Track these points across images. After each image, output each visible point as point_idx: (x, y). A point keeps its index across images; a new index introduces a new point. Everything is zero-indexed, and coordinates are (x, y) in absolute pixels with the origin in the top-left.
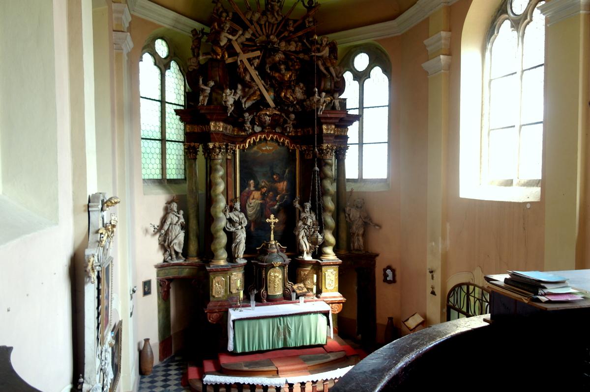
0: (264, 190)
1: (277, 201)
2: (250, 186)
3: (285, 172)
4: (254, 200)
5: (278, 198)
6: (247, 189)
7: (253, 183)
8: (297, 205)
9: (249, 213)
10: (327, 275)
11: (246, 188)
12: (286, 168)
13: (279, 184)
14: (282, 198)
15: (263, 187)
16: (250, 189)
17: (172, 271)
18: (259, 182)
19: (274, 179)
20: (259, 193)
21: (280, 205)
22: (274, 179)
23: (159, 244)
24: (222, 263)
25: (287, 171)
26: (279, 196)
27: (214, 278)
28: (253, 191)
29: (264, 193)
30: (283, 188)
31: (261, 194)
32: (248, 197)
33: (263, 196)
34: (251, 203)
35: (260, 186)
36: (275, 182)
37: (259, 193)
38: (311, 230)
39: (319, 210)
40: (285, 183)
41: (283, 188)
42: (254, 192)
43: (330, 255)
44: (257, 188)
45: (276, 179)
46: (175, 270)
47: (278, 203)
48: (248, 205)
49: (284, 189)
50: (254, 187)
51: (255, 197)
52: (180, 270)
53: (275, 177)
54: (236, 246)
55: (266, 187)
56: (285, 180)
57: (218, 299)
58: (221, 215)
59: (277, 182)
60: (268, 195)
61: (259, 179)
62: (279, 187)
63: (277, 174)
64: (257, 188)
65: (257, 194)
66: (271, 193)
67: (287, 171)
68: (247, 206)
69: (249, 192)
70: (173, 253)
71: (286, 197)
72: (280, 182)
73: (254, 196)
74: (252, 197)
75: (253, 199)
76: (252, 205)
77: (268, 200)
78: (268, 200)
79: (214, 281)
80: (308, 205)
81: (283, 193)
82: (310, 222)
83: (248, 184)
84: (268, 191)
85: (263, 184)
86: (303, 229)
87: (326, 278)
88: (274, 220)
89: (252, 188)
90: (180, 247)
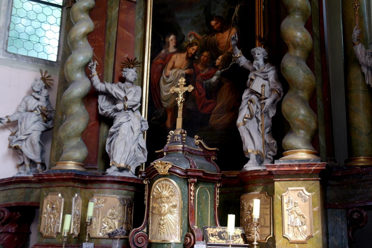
0: (192, 50)
1: (217, 68)
2: (169, 46)
3: (232, 11)
4: (174, 71)
5: (218, 62)
6: (163, 51)
7: (174, 40)
9: (165, 94)
10: (285, 200)
11: (161, 50)
12: (236, 5)
15: (191, 45)
16: (168, 51)
17: (18, 192)
18: (184, 36)
19: (211, 27)
20: (184, 55)
21: (222, 75)
22: (213, 27)
23: (10, 147)
24: (71, 166)
25: (237, 9)
26: (220, 57)
27: (47, 195)
28: (174, 53)
29: (193, 55)
31: (188, 58)
32: (164, 66)
33: (191, 60)
34: (168, 77)
35: (185, 44)
36: (212, 31)
37: (184, 55)
38: (264, 103)
39: (277, 53)
40: (234, 31)
42: (174, 56)
43: (301, 154)
44: (180, 48)
45: (215, 28)
46: (22, 191)
47: (218, 72)
48: (164, 81)
50: (176, 47)
51: (176, 64)
52: (28, 190)
53: (213, 23)
54: (111, 141)
55: (197, 45)
56: (233, 26)
57: (49, 241)
58: (79, 75)
59: (219, 32)
60: (199, 57)
61: (184, 33)
62: (221, 41)
63: (217, 17)
64: (180, 48)
65: (179, 59)
66: (205, 54)
67: (237, 9)
68: (161, 82)
69: (167, 55)
70: (27, 163)
72: (222, 32)
73: (174, 62)
74: (170, 65)
75: (173, 67)
76: (169, 80)
77: (199, 67)
78: (199, 67)
79: (45, 201)
82: (262, 86)
83: (164, 42)
84: (201, 50)
85: (191, 40)
87: (285, 207)
88: (186, 89)
89: (172, 49)
90: (34, 151)
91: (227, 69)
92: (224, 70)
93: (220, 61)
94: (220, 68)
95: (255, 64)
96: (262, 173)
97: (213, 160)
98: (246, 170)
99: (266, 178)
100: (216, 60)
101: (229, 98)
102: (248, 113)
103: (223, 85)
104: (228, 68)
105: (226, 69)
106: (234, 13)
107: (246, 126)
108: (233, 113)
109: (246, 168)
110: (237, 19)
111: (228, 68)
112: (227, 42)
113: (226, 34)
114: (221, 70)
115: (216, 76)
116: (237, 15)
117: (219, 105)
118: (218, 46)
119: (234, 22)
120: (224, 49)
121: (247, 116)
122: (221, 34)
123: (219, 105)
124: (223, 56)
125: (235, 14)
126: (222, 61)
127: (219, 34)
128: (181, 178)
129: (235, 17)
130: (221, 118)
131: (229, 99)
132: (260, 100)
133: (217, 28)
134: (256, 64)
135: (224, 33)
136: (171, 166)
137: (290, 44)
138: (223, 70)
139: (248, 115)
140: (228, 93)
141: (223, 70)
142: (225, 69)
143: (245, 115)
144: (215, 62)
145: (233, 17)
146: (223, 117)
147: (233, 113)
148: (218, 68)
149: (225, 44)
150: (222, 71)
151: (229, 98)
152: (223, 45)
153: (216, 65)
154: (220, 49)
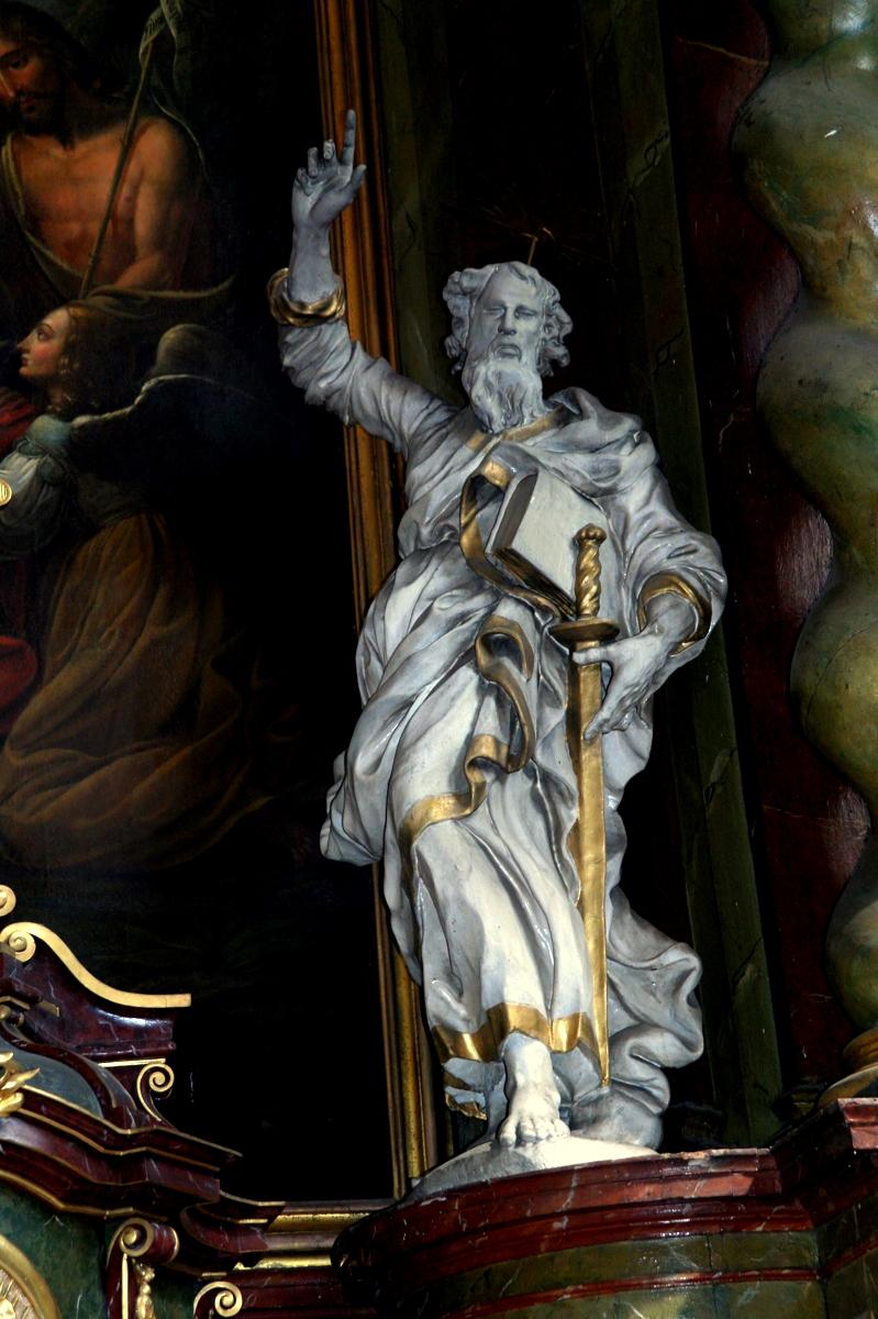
1: (34, 395)
5: (39, 350)
8: (341, 368)
13: (49, 157)
14: (111, 353)
21: (78, 453)
26: (58, 319)
30: (118, 222)
38: (609, 672)
40: (156, 145)
41: (118, 222)
47: (47, 427)
49: (143, 227)
56: (150, 110)
59: (38, 129)
62: (63, 199)
71: (170, 337)
80: (518, 306)
81: (129, 279)
82: (579, 543)
86: (465, 656)
91: (118, 413)
92: (96, 418)
93: (55, 344)
94: (59, 396)
95: (488, 385)
96: (700, 1183)
97: (155, 1094)
98: (524, 1161)
99: (716, 1229)
100: (27, 334)
101: (150, 632)
102: (490, 724)
103: (91, 529)
104: (128, 410)
105: (108, 415)
106: (154, 16)
107: (479, 822)
108: (187, 751)
109: (528, 1152)
110: (178, 64)
111: (128, 410)
112: (111, 214)
113: (98, 156)
114: (67, 416)
115: (30, 454)
116: (173, 32)
117: (62, 682)
118: (37, 233)
119: (156, 81)
120: (90, 262)
121: (486, 750)
122: (58, 152)
123: (62, 682)
124: (79, 312)
125: (162, 19)
126: (69, 348)
127: (36, 141)
128: (62, 1214)
129: (163, 39)
130: (86, 784)
131: (142, 642)
132: (567, 638)
133: (19, 93)
134: (492, 379)
135: (82, 148)
136: (19, 1098)
137: (857, 254)
138: (81, 420)
139: (497, 743)
140: (136, 599)
141: (81, 420)
142: (100, 412)
143: (471, 741)
144: (21, 351)
145: (146, 42)
146: (102, 773)
147: (187, 751)
148: (47, 399)
149: (95, 228)
150: (82, 427)
151: (150, 632)
152: (75, 228)
153: (23, 370)
154: (48, 253)
